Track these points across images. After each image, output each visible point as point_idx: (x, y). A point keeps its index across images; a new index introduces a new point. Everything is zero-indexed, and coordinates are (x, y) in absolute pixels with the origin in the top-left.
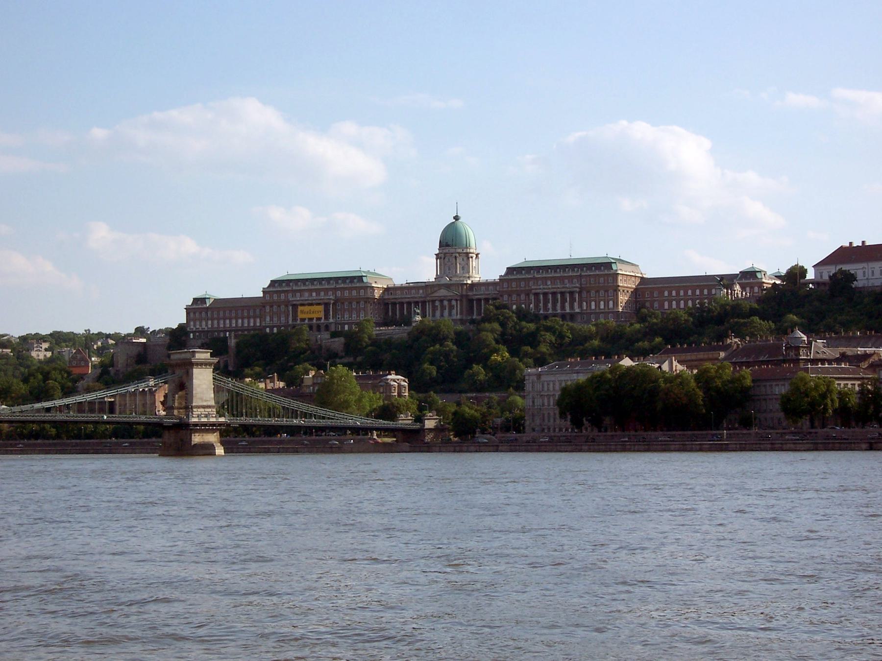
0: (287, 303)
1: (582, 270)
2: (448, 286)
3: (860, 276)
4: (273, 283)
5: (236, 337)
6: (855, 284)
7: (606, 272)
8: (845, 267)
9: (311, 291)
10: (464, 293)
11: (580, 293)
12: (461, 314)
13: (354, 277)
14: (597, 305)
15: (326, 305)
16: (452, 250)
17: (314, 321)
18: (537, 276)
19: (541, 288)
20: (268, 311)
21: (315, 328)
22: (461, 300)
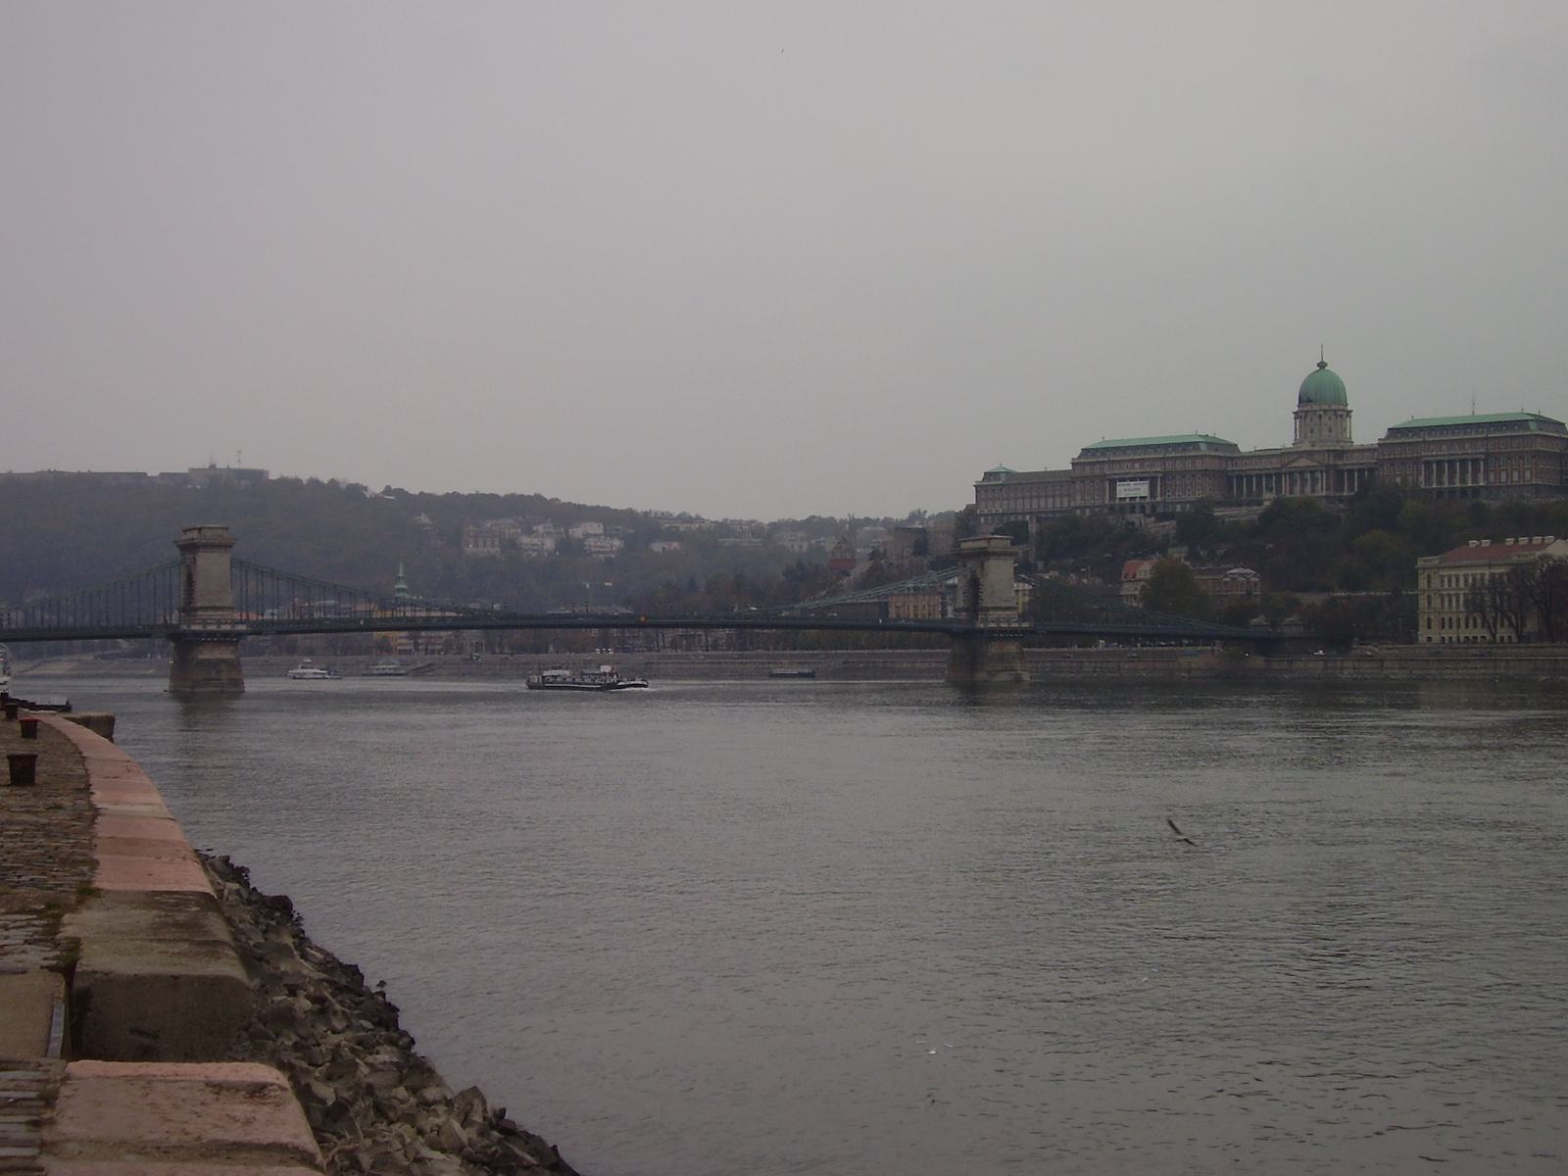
0: (1103, 478)
2: (1309, 454)
4: (1086, 451)
5: (1039, 520)
9: (1133, 461)
10: (1331, 462)
11: (1485, 460)
12: (1328, 489)
13: (1189, 444)
15: (1153, 481)
16: (1315, 408)
17: (1138, 500)
18: (1427, 439)
21: (1137, 509)
22: (1327, 472)
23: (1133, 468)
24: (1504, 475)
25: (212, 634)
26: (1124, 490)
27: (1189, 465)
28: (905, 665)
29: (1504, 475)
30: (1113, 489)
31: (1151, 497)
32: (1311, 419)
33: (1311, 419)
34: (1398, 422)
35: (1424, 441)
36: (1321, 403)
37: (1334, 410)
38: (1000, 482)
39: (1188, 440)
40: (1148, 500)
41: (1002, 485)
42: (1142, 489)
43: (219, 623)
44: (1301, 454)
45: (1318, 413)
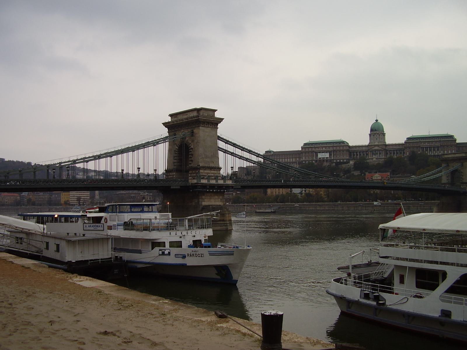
0: (312, 152)
1: (441, 139)
2: (378, 146)
4: (305, 144)
7: (451, 139)
10: (385, 148)
12: (384, 156)
13: (341, 142)
15: (330, 152)
16: (378, 132)
17: (325, 158)
18: (421, 141)
19: (422, 145)
23: (323, 149)
25: (212, 187)
26: (320, 156)
27: (341, 148)
28: (311, 208)
30: (317, 155)
31: (330, 157)
32: (377, 136)
33: (377, 136)
35: (420, 142)
36: (377, 131)
37: (383, 133)
38: (272, 154)
39: (330, 142)
40: (329, 158)
41: (272, 155)
42: (327, 155)
43: (209, 178)
44: (375, 146)
45: (379, 134)
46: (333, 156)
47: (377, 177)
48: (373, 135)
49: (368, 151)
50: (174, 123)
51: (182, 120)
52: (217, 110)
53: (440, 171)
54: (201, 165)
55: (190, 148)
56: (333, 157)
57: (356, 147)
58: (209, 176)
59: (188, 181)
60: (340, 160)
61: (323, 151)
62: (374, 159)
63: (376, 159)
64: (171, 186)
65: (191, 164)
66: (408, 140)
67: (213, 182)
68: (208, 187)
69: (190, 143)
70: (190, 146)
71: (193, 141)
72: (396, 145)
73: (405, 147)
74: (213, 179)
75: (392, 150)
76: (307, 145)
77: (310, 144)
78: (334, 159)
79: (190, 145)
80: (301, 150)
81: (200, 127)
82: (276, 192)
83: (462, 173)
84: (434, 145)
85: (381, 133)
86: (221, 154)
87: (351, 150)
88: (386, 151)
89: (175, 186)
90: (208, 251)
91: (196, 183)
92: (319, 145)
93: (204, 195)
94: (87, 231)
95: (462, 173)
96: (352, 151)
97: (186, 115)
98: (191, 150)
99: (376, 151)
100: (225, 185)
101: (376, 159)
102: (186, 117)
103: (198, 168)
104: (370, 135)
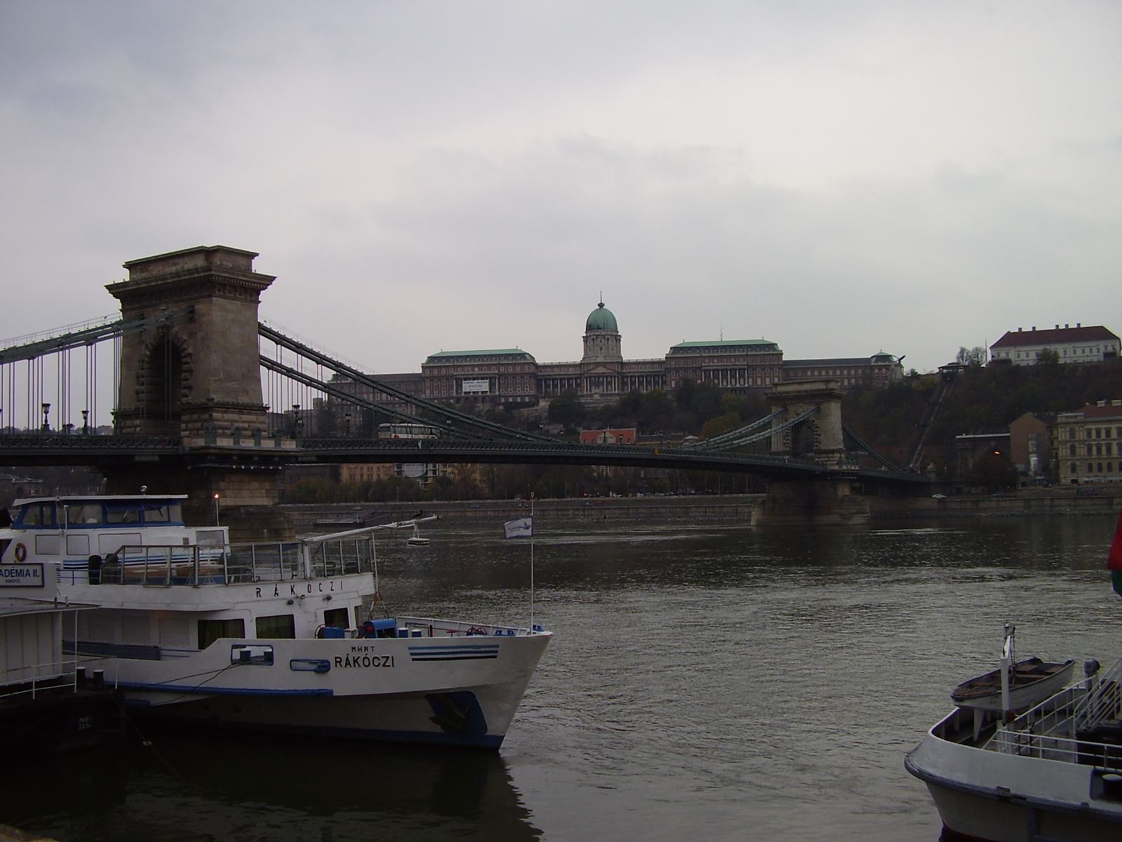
0: (449, 378)
1: (748, 351)
2: (604, 364)
3: (1061, 354)
4: (431, 359)
6: (1061, 361)
7: (771, 352)
8: (1052, 348)
9: (474, 366)
10: (619, 370)
12: (618, 389)
13: (519, 355)
14: (763, 381)
15: (491, 379)
16: (603, 333)
19: (706, 364)
20: (428, 384)
23: (474, 370)
24: (759, 381)
25: (246, 456)
26: (468, 387)
27: (518, 370)
28: (452, 514)
29: (759, 381)
30: (459, 386)
32: (601, 341)
33: (601, 341)
34: (677, 343)
35: (701, 356)
36: (601, 330)
37: (616, 336)
40: (488, 394)
42: (484, 386)
43: (237, 434)
44: (598, 364)
46: (499, 388)
47: (609, 437)
48: (593, 340)
49: (580, 378)
50: (140, 286)
51: (163, 277)
52: (257, 255)
53: (767, 426)
54: (217, 398)
55: (183, 355)
56: (499, 391)
57: (551, 367)
58: (238, 429)
59: (178, 442)
60: (515, 397)
61: (475, 376)
62: (596, 396)
63: (602, 395)
64: (134, 456)
65: (187, 396)
66: (673, 353)
67: (248, 444)
68: (236, 458)
69: (185, 340)
70: (185, 349)
71: (192, 335)
72: (645, 363)
73: (666, 369)
74: (246, 437)
75: (637, 374)
76: (436, 361)
77: (443, 357)
78: (500, 396)
79: (184, 346)
80: (421, 372)
81: (214, 298)
82: (362, 475)
83: (818, 427)
84: (733, 365)
85: (610, 335)
86: (263, 369)
87: (541, 374)
88: (623, 377)
89: (148, 454)
90: (410, 648)
91: (203, 448)
92: (466, 360)
93: (224, 480)
94: (30, 590)
95: (817, 429)
96: (543, 376)
97: (175, 264)
98: (188, 359)
99: (599, 377)
100: (279, 454)
101: (602, 395)
102: (173, 269)
103: (206, 408)
104: (586, 339)
